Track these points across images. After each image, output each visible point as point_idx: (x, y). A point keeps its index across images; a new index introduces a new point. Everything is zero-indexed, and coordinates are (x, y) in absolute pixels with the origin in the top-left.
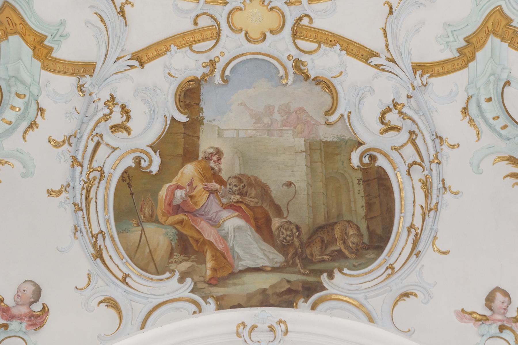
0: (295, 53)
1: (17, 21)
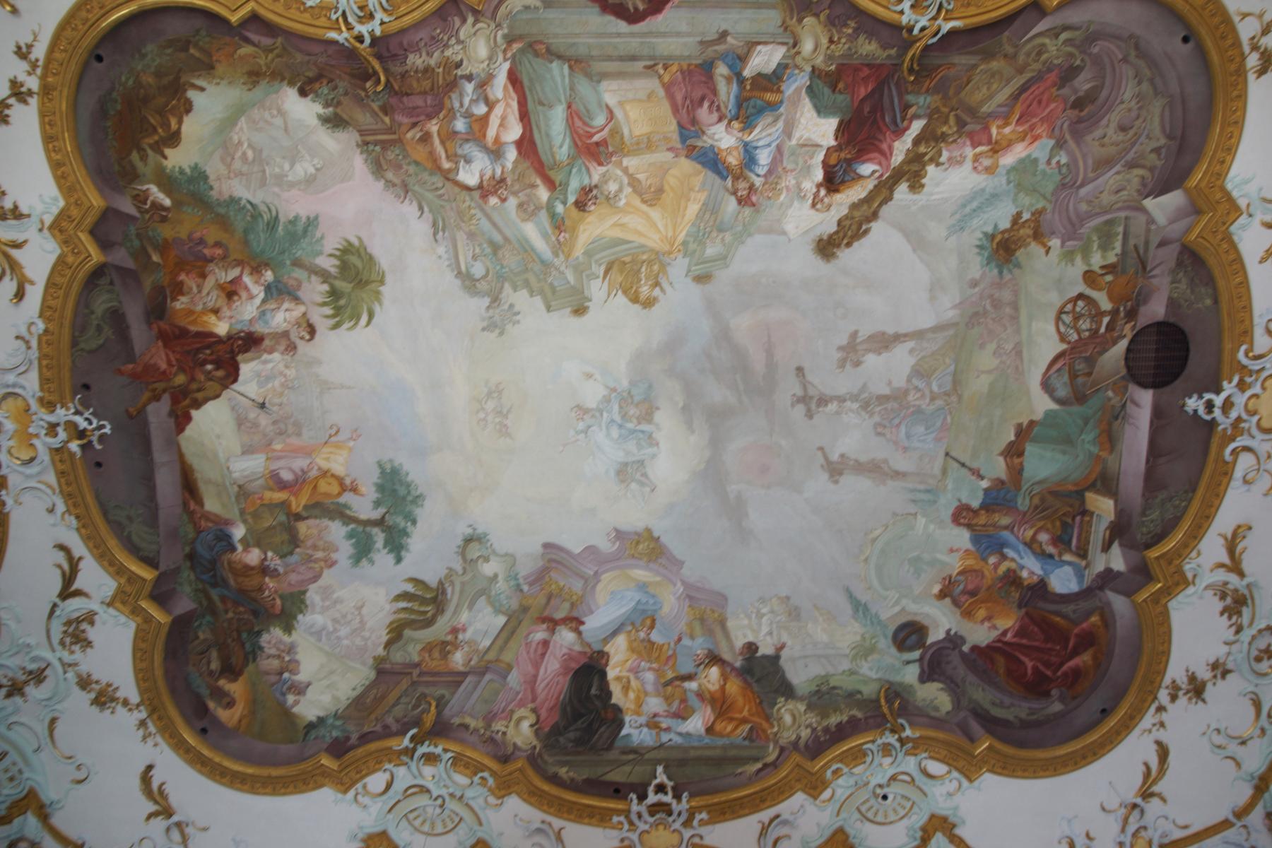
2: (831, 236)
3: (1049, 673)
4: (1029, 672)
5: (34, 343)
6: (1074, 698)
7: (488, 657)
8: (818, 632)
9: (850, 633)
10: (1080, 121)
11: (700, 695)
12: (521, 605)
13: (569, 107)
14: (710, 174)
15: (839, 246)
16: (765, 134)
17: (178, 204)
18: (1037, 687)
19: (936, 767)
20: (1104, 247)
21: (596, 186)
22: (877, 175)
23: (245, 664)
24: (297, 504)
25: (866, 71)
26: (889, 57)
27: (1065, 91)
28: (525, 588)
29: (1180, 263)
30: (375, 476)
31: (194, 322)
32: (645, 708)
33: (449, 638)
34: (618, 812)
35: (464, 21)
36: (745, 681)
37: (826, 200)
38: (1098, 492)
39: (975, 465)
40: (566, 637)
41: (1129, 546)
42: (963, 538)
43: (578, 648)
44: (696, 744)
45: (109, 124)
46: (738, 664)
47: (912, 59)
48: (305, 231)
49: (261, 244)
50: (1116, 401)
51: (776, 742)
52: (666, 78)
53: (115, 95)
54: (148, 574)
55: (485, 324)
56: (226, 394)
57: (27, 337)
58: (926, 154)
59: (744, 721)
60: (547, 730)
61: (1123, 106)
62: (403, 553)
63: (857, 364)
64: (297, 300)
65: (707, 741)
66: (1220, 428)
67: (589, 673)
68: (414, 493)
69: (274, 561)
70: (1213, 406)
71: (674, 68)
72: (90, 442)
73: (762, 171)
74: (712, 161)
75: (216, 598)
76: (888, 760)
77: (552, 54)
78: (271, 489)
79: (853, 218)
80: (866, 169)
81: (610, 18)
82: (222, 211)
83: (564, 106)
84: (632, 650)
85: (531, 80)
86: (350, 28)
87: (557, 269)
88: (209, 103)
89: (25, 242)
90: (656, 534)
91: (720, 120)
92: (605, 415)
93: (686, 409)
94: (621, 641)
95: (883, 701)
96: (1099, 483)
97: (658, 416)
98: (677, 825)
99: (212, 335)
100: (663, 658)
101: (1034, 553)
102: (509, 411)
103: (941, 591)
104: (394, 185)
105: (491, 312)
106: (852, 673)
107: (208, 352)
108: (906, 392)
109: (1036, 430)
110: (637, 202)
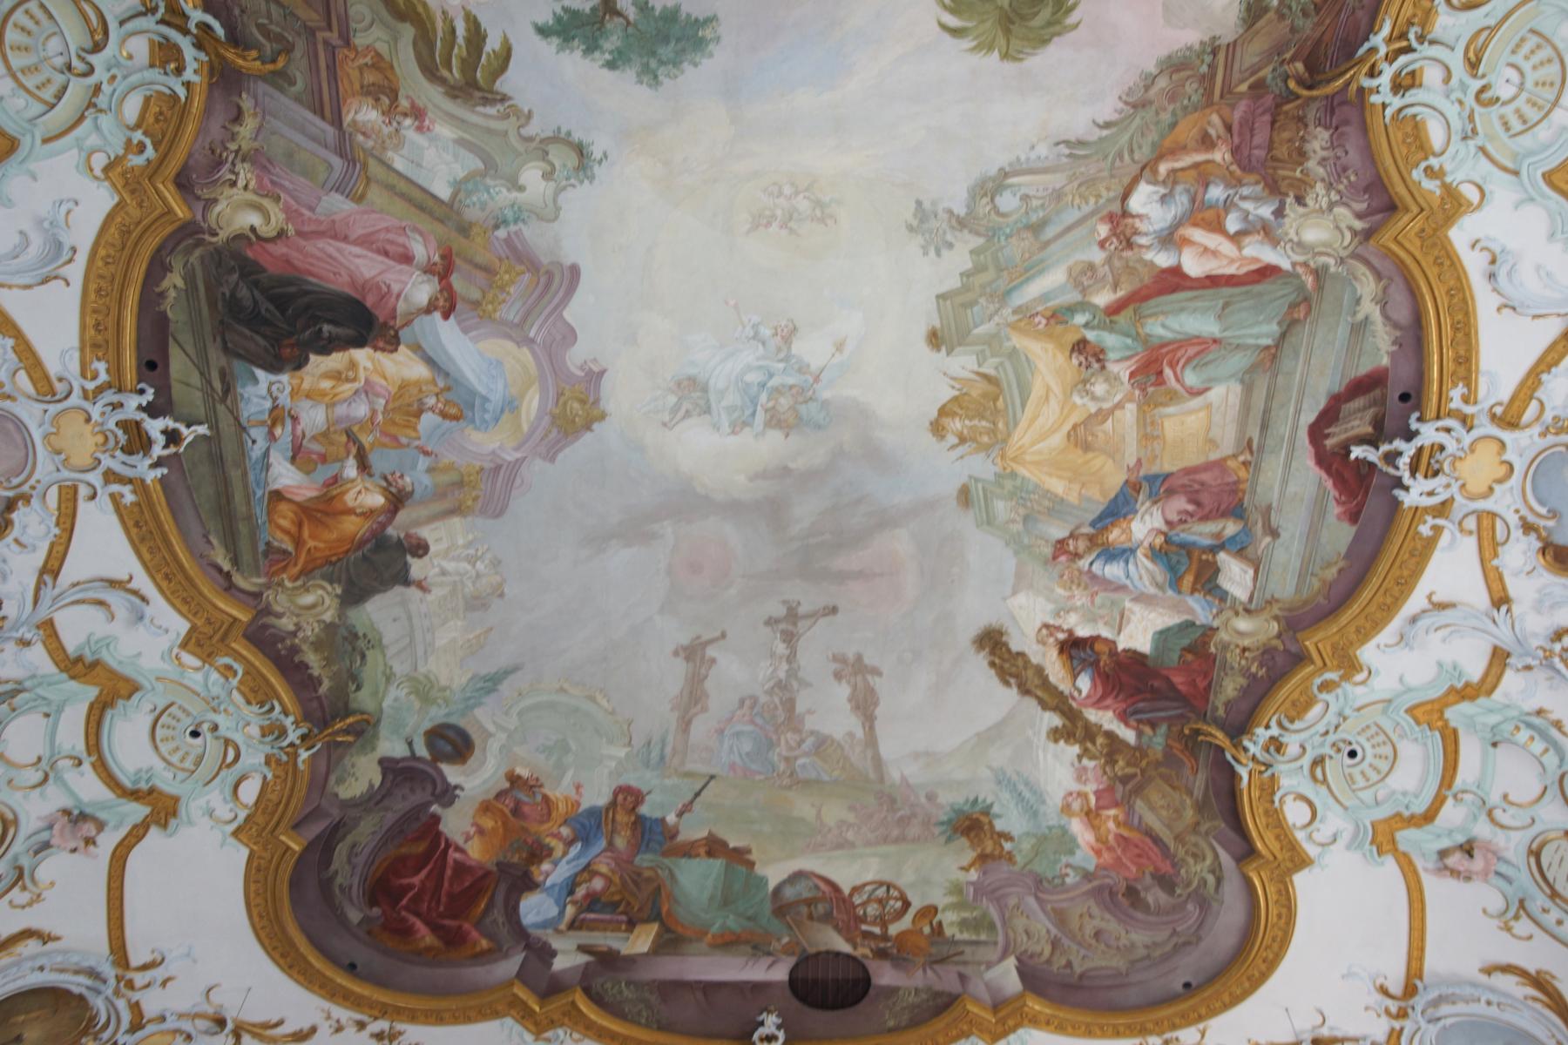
0: (1537, 429)
1: (1429, 707)
2: (1006, 645)
3: (404, 902)
4: (405, 881)
6: (369, 933)
7: (372, 162)
8: (451, 633)
9: (449, 672)
10: (1112, 894)
11: (335, 480)
12: (471, 225)
13: (1215, 341)
14: (1101, 508)
15: (992, 653)
16: (1143, 572)
18: (382, 889)
19: (250, 791)
20: (964, 924)
21: (1103, 368)
22: (1076, 694)
25: (1202, 684)
26: (1216, 709)
27: (1148, 879)
28: (501, 233)
29: (937, 994)
32: (306, 404)
33: (404, 103)
34: (116, 369)
36: (362, 543)
37: (1051, 640)
38: (658, 935)
39: (697, 806)
40: (422, 290)
41: (586, 973)
42: (597, 796)
43: (401, 307)
44: (251, 477)
46: (390, 531)
47: (1211, 735)
50: (775, 946)
51: (268, 586)
52: (1231, 463)
55: (927, 205)
58: (1094, 743)
59: (298, 542)
60: (250, 254)
61: (1123, 933)
62: (555, 41)
63: (838, 676)
65: (259, 493)
67: (362, 322)
68: (661, 71)
71: (1242, 474)
73: (1096, 568)
74: (1118, 510)
76: (254, 731)
77: (1289, 326)
79: (1025, 668)
80: (1085, 683)
81: (1322, 404)
83: (1218, 335)
84: (404, 386)
85: (1260, 294)
86: (1391, 58)
87: (996, 312)
90: (595, 426)
91: (1168, 523)
92: (781, 366)
93: (786, 471)
94: (419, 371)
96: (667, 936)
97: (775, 436)
98: (107, 462)
100: (393, 430)
101: (576, 875)
102: (791, 231)
103: (519, 777)
104: (1147, 88)
105: (943, 216)
106: (389, 677)
108: (797, 730)
109: (743, 869)
110: (1076, 418)
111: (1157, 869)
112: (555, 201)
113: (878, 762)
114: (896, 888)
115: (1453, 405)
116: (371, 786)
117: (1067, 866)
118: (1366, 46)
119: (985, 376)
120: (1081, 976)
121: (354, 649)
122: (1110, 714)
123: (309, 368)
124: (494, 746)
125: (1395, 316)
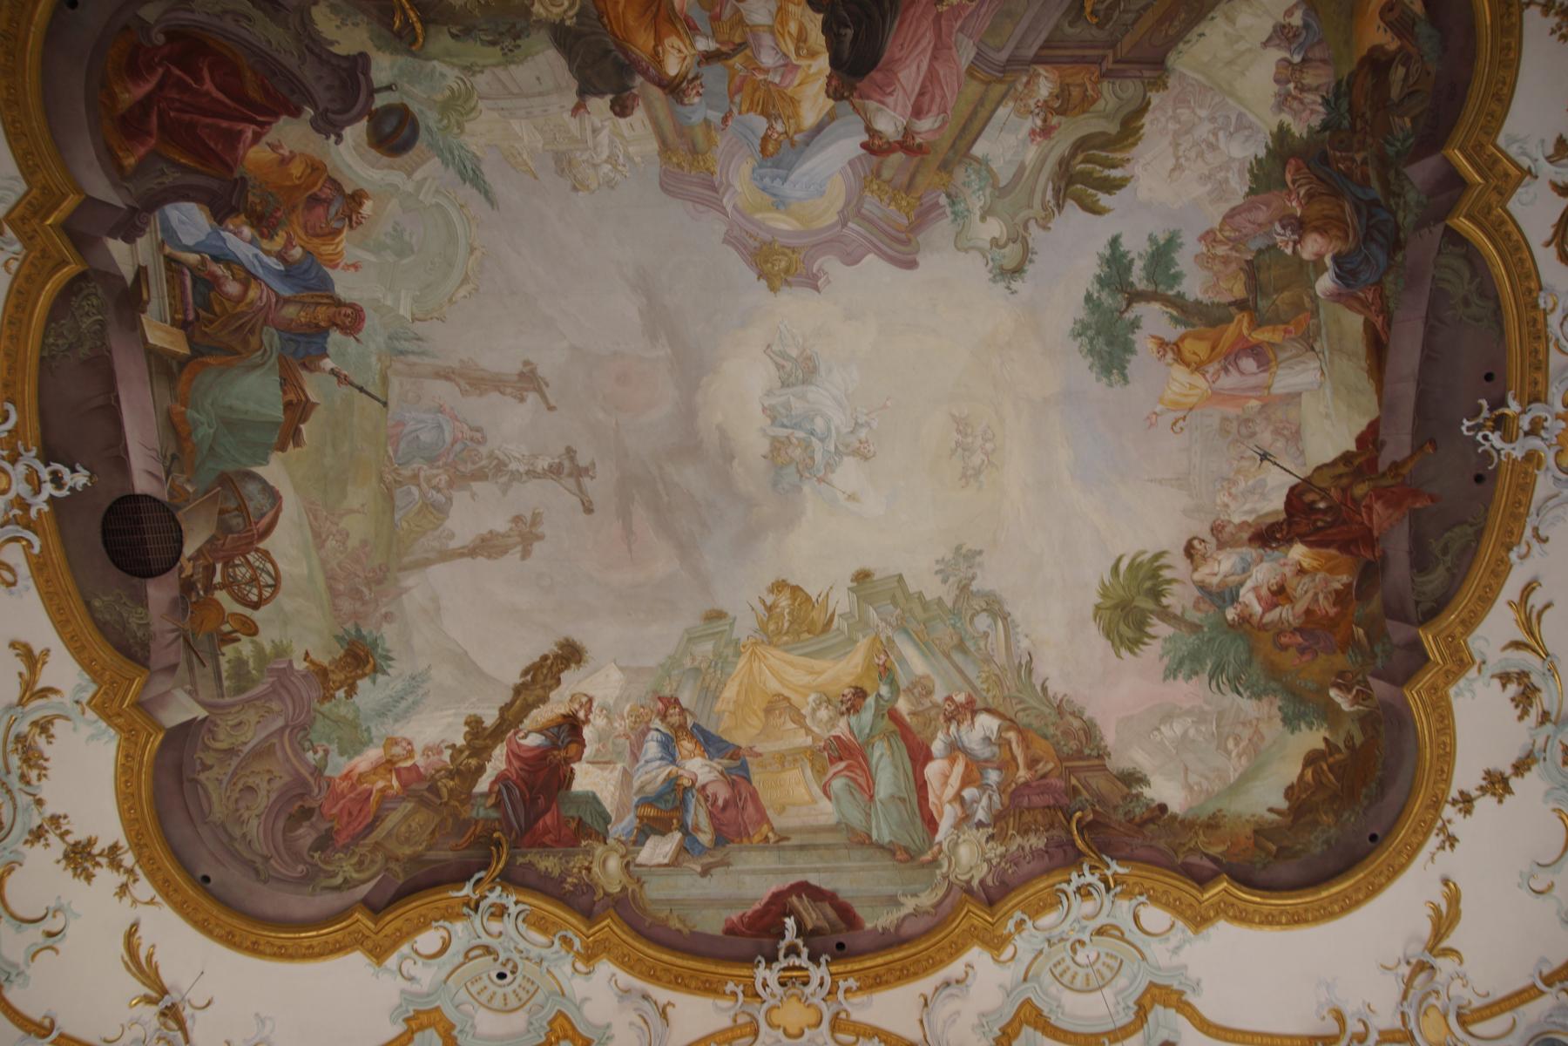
1: (567, 1026)
2: (567, 667)
3: (177, 72)
5: (1528, 532)
8: (527, 136)
9: (481, 132)
10: (301, 796)
11: (692, 29)
12: (950, 173)
13: (872, 797)
14: (713, 731)
15: (556, 657)
16: (653, 772)
17: (1322, 691)
20: (239, 664)
21: (842, 714)
23: (1353, 75)
24: (1242, 321)
25: (547, 839)
26: (524, 855)
27: (324, 826)
28: (943, 200)
29: (145, 646)
30: (1134, 364)
31: (1330, 558)
33: (1055, 120)
35: (982, 882)
36: (626, 53)
38: (174, 355)
39: (345, 389)
40: (888, 124)
41: (110, 277)
42: (345, 286)
43: (872, 105)
45: (1379, 773)
46: (639, 80)
47: (499, 858)
48: (1181, 663)
49: (1238, 649)
50: (181, 479)
52: (765, 828)
53: (1365, 803)
54: (1463, 224)
55: (978, 559)
56: (1306, 472)
57: (1534, 542)
62: (1107, 252)
63: (517, 519)
64: (1202, 586)
66: (33, 453)
67: (856, 66)
69: (1283, 239)
70: (52, 481)
71: (757, 838)
72: (1491, 409)
74: (710, 743)
75: (1375, 184)
77: (889, 850)
78: (1271, 345)
79: (543, 687)
80: (534, 740)
81: (826, 887)
82: (1273, 685)
83: (876, 798)
84: (794, 102)
85: (913, 823)
86: (1105, 881)
88: (1266, 797)
89: (1505, 648)
90: (763, 282)
91: (704, 787)
92: (832, 449)
94: (809, 117)
95: (418, 26)
96: (175, 365)
97: (764, 446)
99: (1310, 544)
100: (748, 89)
101: (241, 265)
102: (954, 452)
103: (361, 204)
104: (1073, 714)
106: (469, 69)
107: (1320, 524)
109: (275, 439)
110: (794, 698)
111: (338, 832)
112: (972, 248)
113: (426, 563)
114: (273, 594)
115: (841, 983)
116: (332, 43)
117: (326, 752)
118: (1108, 860)
119: (831, 620)
120: (197, 782)
121: (501, 34)
122: (503, 766)
123: (809, 11)
124: (397, 177)
125: (906, 924)
